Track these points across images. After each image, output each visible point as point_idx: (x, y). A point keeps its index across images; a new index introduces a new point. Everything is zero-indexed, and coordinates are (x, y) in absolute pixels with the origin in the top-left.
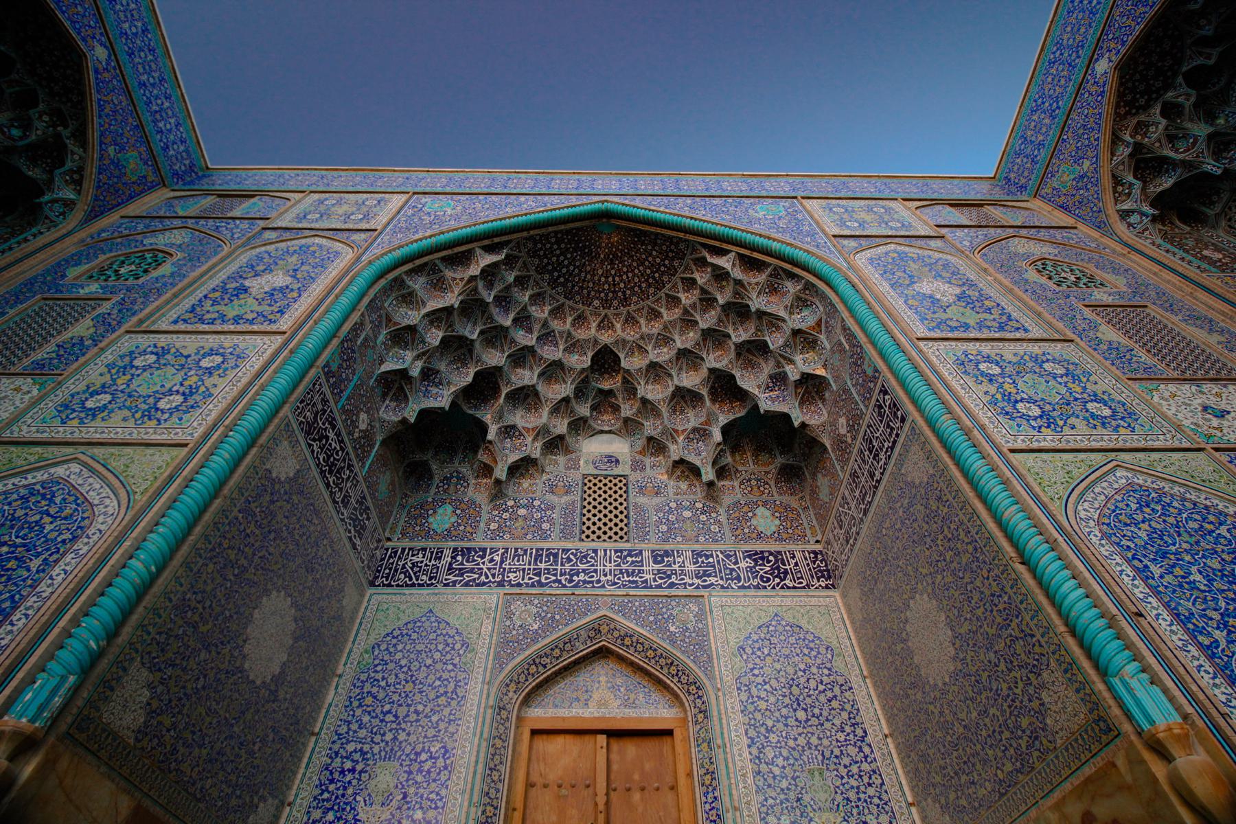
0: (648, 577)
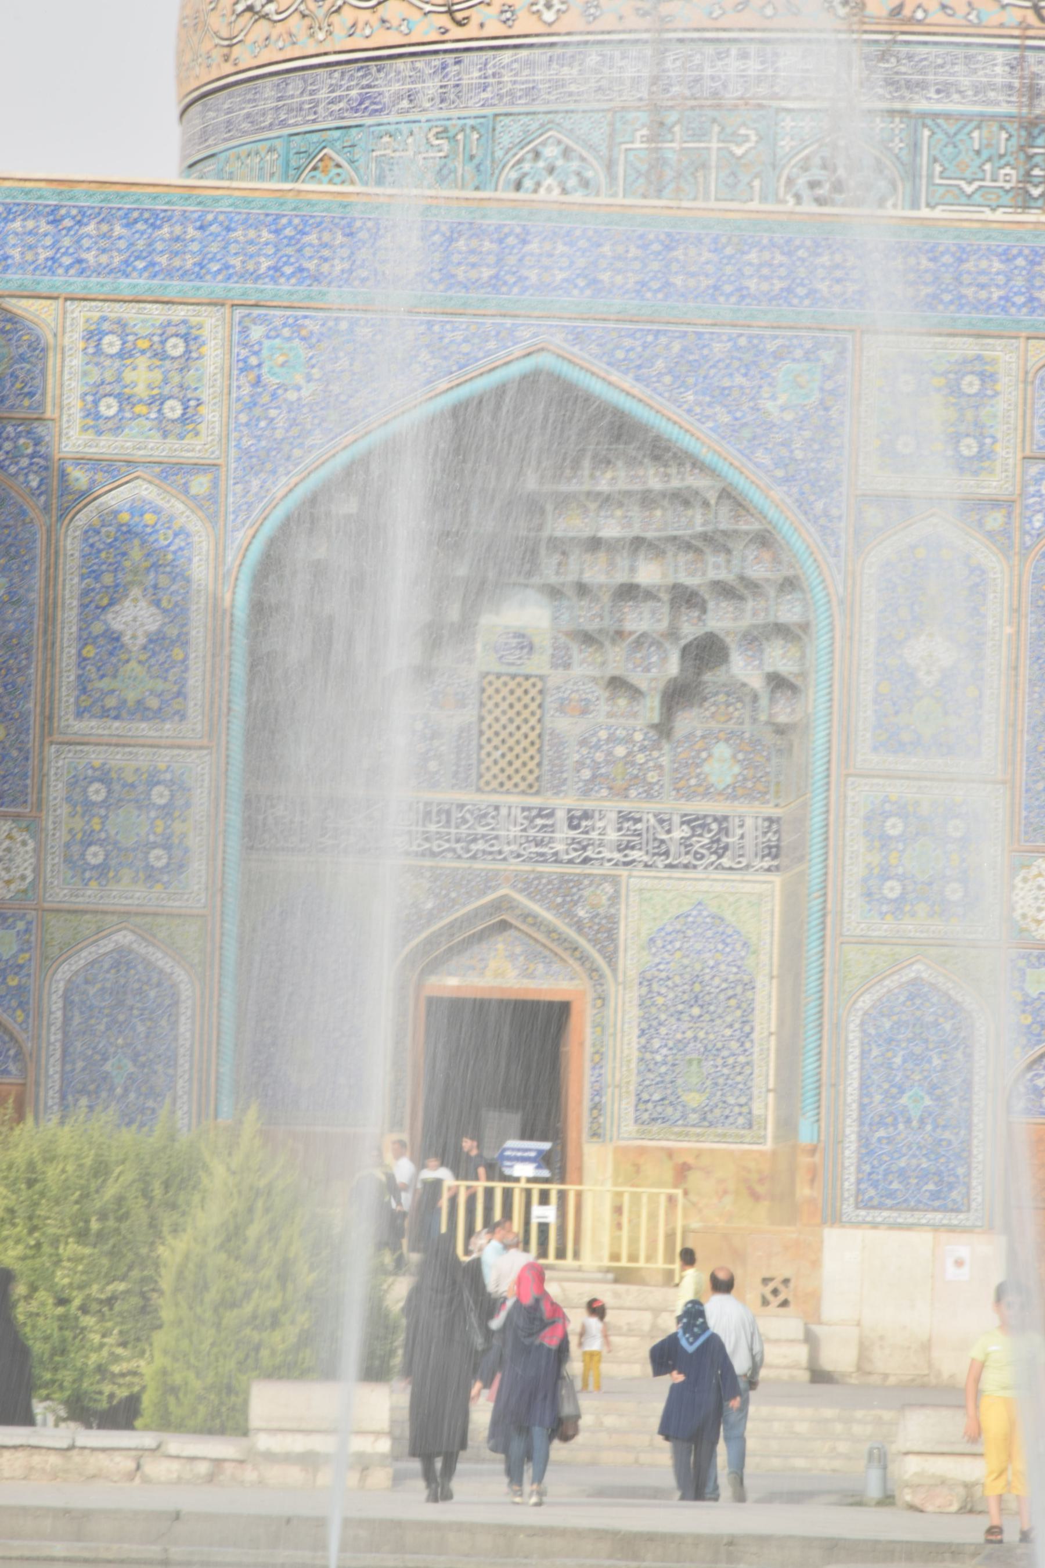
0: (560, 847)
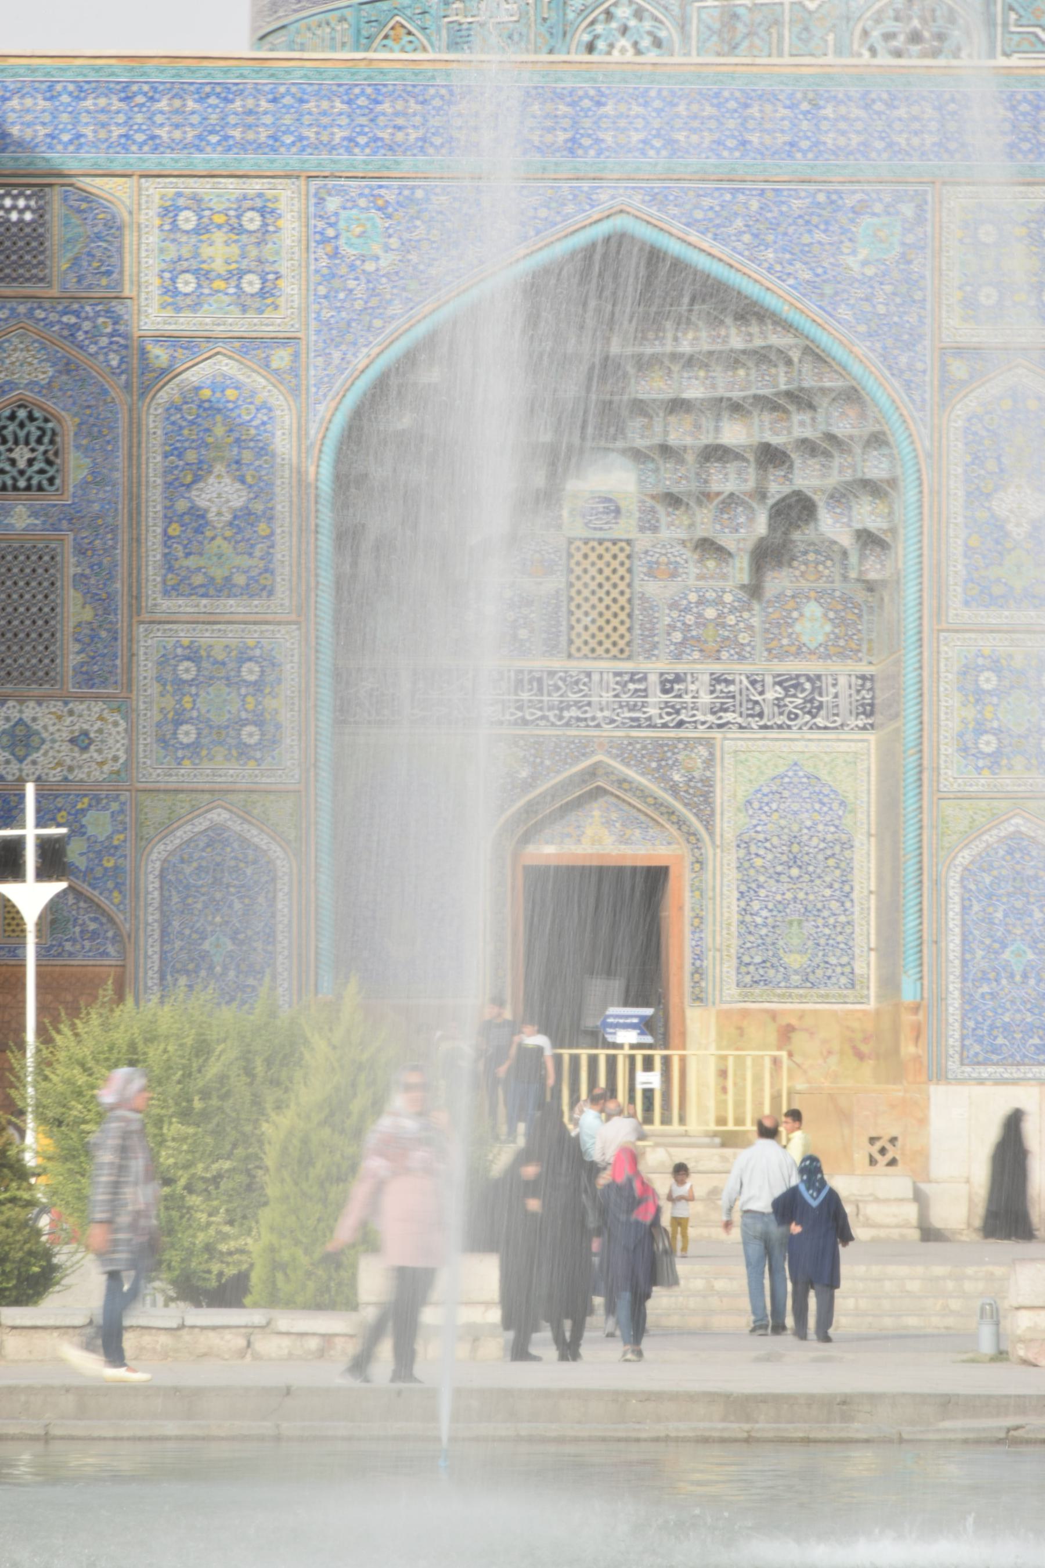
0: (653, 711)
